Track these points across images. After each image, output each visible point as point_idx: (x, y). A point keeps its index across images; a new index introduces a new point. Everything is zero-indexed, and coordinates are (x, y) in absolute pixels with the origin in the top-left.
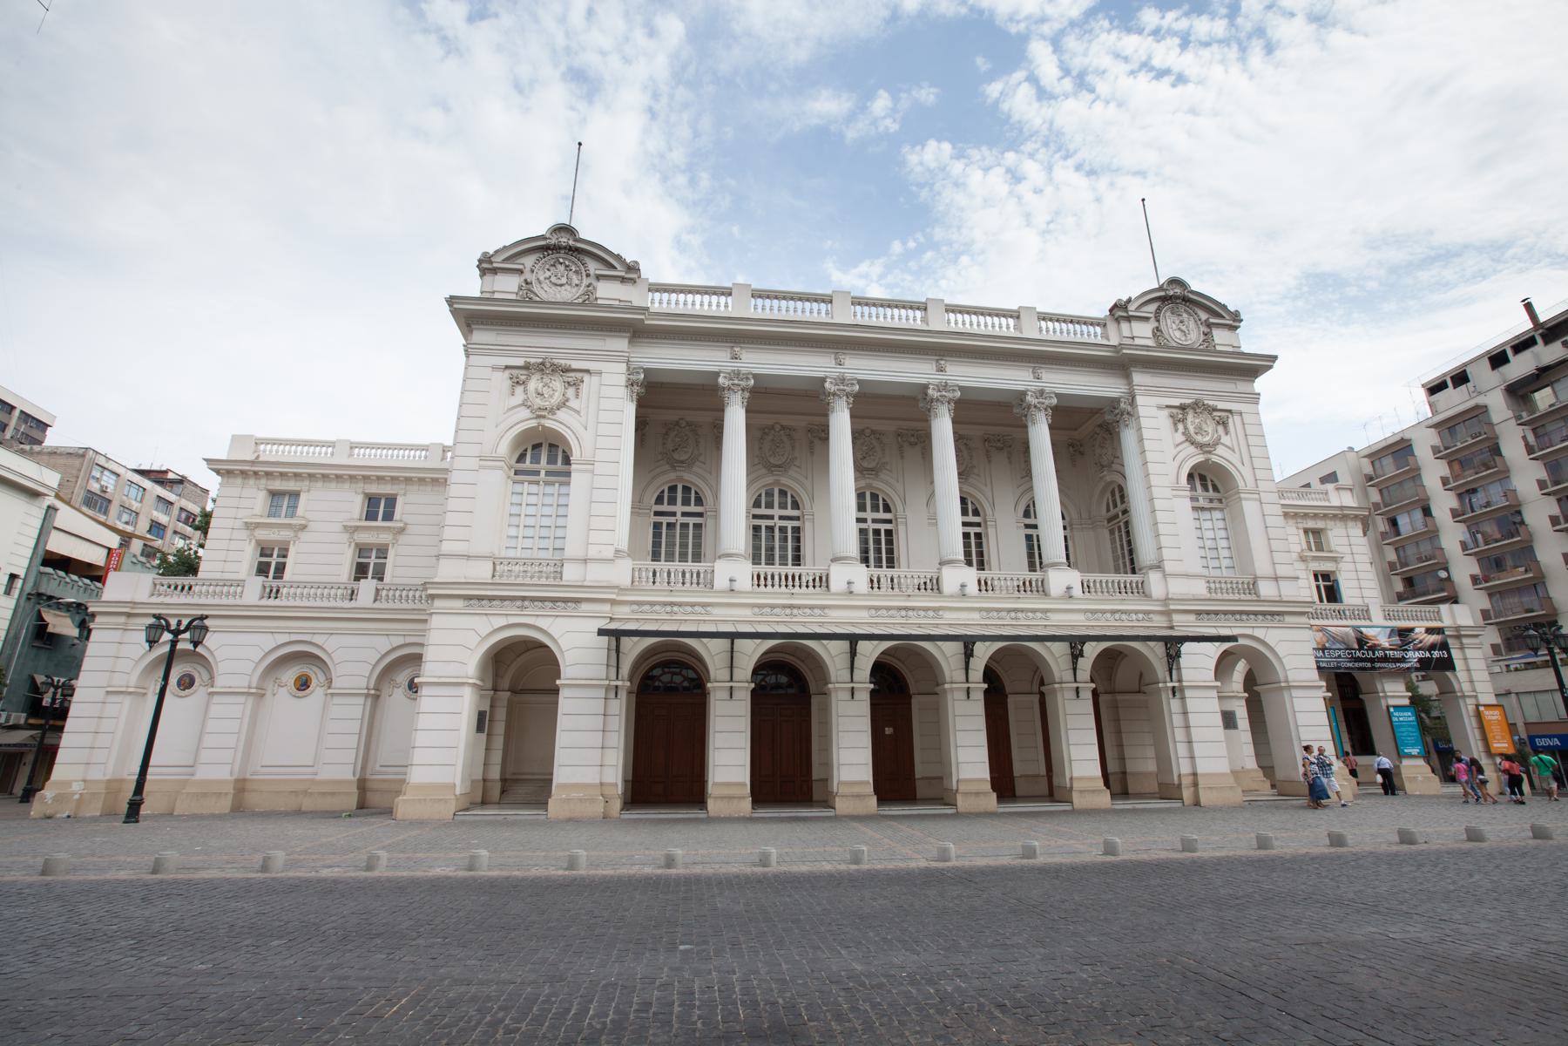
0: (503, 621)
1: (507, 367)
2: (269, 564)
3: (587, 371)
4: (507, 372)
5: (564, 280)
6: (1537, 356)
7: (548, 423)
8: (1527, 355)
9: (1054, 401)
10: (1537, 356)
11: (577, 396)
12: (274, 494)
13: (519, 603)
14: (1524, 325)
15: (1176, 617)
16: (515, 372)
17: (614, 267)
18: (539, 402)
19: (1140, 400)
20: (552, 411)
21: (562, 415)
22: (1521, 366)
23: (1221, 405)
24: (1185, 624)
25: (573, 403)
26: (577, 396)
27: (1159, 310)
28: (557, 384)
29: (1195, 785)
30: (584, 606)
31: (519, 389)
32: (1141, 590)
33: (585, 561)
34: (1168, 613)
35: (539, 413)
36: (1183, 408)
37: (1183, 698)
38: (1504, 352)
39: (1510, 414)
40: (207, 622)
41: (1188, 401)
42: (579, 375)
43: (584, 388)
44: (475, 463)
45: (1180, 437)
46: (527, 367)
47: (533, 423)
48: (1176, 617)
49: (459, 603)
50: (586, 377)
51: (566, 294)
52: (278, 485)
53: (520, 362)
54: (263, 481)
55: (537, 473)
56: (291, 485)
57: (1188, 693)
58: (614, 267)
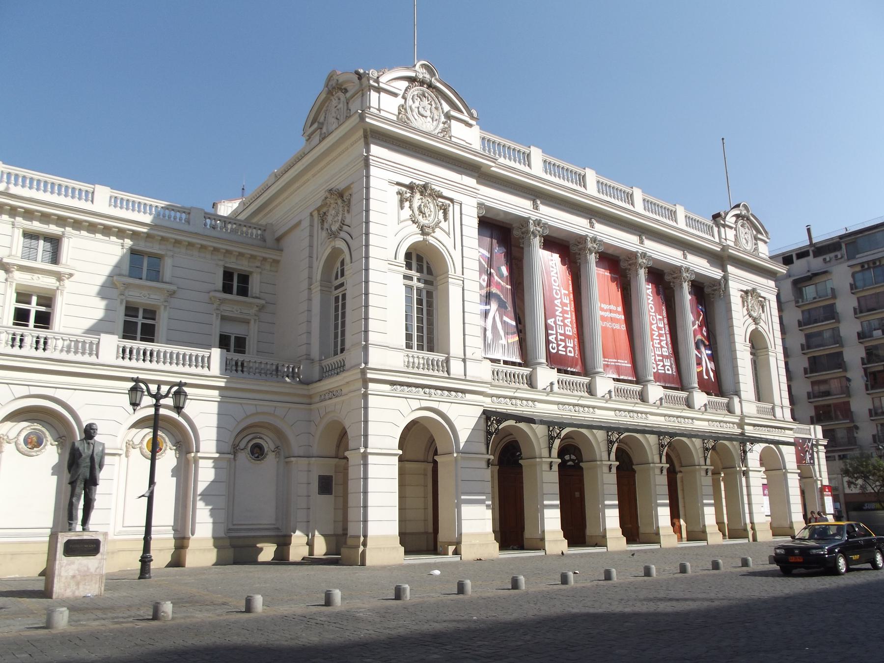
1: (398, 184)
2: (27, 312)
3: (452, 200)
5: (428, 113)
6: (808, 263)
7: (430, 239)
8: (803, 261)
9: (693, 277)
10: (808, 263)
11: (446, 219)
12: (30, 235)
14: (802, 241)
15: (746, 427)
16: (404, 189)
17: (461, 112)
19: (731, 284)
21: (438, 233)
22: (801, 267)
23: (763, 294)
24: (749, 431)
25: (444, 225)
26: (446, 219)
27: (736, 222)
28: (431, 207)
29: (753, 528)
32: (730, 410)
33: (464, 360)
34: (741, 425)
35: (423, 230)
36: (746, 292)
37: (747, 478)
38: (791, 256)
39: (793, 298)
40: (185, 389)
41: (750, 288)
42: (448, 202)
44: (385, 266)
45: (746, 312)
46: (411, 187)
47: (420, 238)
48: (746, 427)
49: (387, 387)
51: (427, 125)
52: (36, 226)
53: (407, 181)
54: (19, 219)
56: (53, 229)
57: (751, 473)
58: (461, 112)
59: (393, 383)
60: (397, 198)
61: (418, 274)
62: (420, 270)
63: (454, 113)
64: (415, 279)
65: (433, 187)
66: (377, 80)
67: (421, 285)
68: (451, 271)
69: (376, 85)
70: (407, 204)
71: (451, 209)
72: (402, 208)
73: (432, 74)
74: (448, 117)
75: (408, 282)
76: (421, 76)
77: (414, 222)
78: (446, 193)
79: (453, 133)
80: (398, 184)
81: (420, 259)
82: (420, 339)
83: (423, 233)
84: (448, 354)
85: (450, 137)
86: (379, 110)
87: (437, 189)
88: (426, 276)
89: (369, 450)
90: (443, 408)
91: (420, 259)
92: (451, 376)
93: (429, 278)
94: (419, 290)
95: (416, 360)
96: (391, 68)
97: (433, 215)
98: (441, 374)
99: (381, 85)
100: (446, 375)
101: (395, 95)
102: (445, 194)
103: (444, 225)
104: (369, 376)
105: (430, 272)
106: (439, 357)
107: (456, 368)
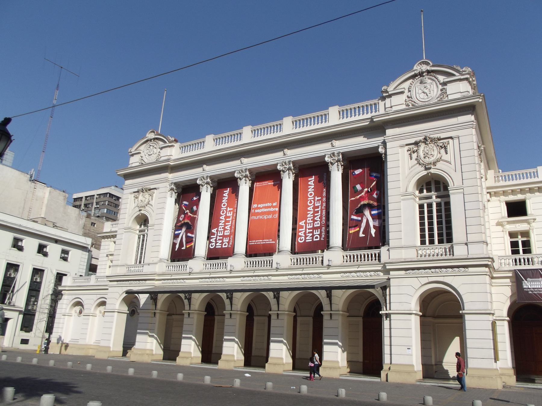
0: (425, 280)
1: (407, 145)
3: (451, 138)
4: (407, 148)
11: (446, 153)
13: (433, 270)
17: (454, 75)
18: (427, 160)
20: (434, 164)
21: (439, 165)
26: (446, 153)
30: (471, 269)
31: (414, 156)
43: (450, 148)
46: (416, 144)
47: (425, 173)
50: (450, 140)
53: (413, 141)
55: (430, 198)
58: (454, 75)
59: (406, 269)
61: (436, 193)
62: (437, 190)
64: (434, 197)
65: (431, 136)
66: (387, 92)
67: (439, 200)
69: (387, 94)
73: (427, 64)
77: (420, 164)
78: (443, 136)
80: (407, 145)
82: (440, 235)
83: (426, 169)
85: (447, 96)
87: (436, 136)
88: (442, 193)
94: (439, 205)
96: (394, 79)
97: (435, 153)
101: (402, 93)
102: (442, 137)
104: (387, 267)
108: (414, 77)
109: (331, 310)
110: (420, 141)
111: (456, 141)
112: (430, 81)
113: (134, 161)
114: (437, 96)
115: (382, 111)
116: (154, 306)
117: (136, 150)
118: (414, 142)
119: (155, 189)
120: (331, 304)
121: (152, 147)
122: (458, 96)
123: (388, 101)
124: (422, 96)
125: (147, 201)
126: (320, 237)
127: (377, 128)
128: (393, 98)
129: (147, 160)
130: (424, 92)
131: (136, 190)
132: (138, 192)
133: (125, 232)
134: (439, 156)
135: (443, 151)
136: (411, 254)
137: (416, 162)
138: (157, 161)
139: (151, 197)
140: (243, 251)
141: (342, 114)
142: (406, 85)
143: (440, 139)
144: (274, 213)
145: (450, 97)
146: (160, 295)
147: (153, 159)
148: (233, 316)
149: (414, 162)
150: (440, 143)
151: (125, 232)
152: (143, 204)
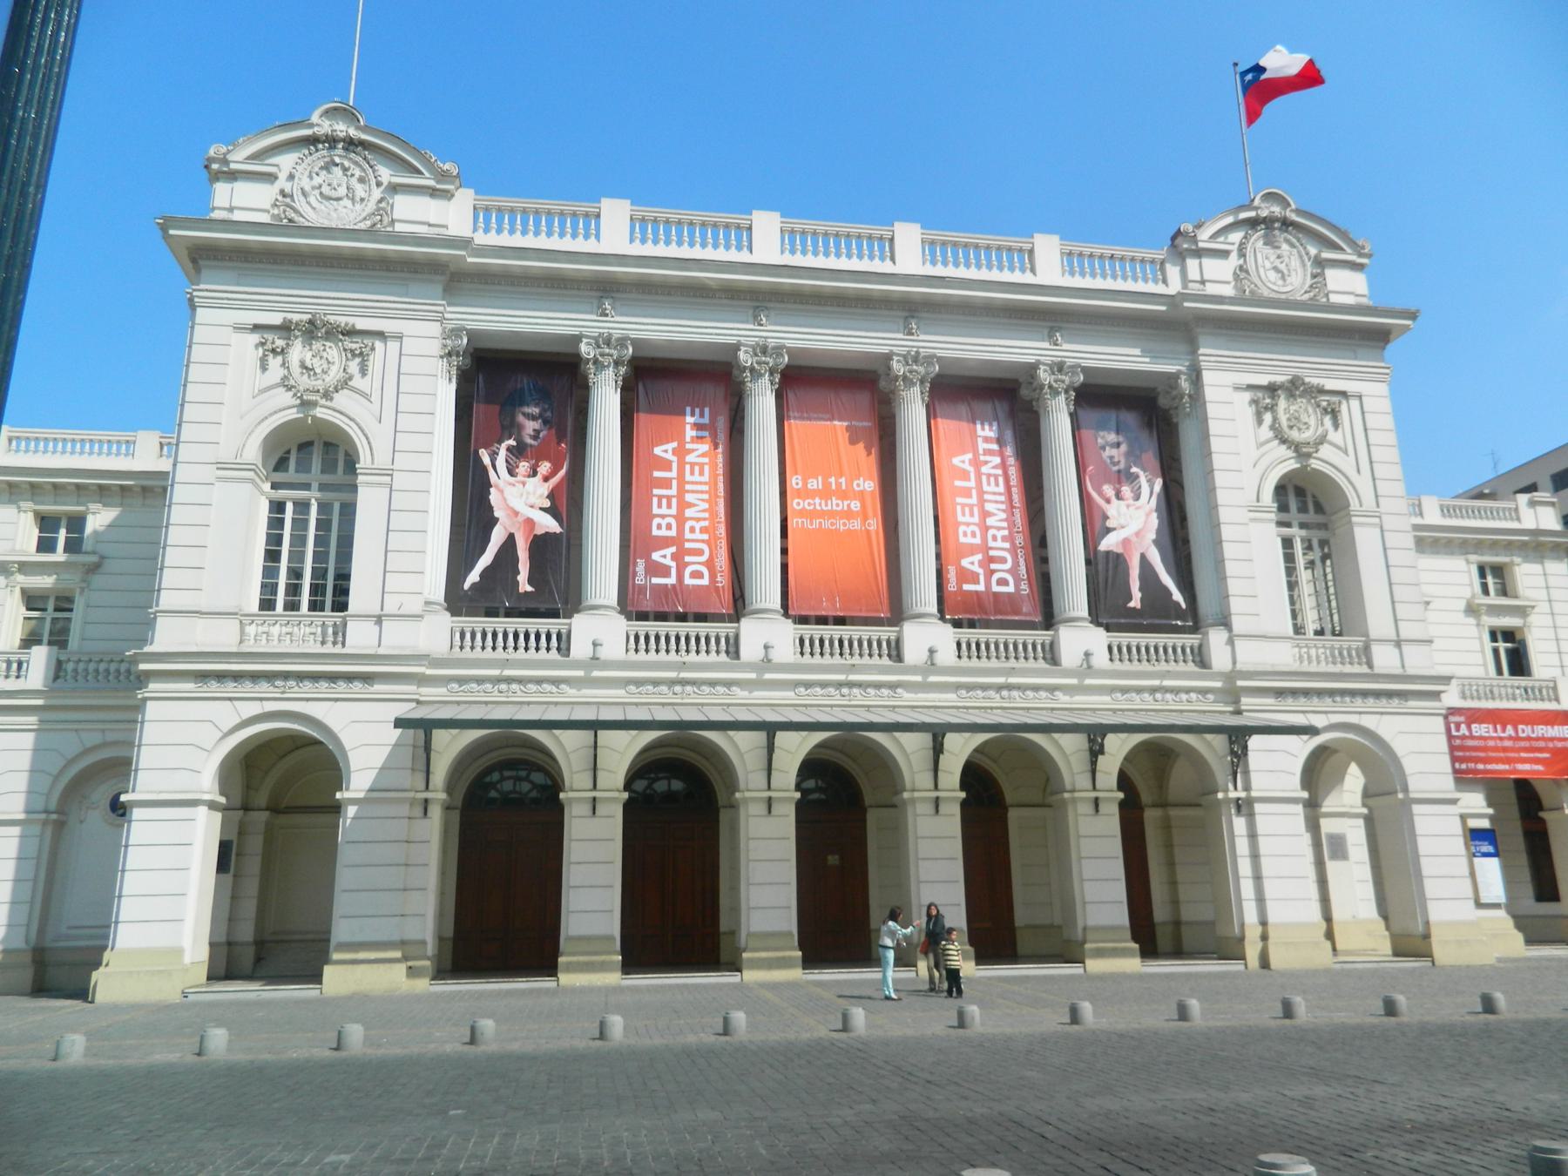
3: (1344, 394)
7: (1315, 464)
11: (1336, 425)
16: (1260, 395)
21: (1325, 451)
42: (1335, 399)
44: (1245, 515)
46: (1272, 389)
47: (1293, 465)
60: (1250, 412)
63: (1327, 255)
68: (1354, 504)
70: (1268, 417)
71: (1344, 407)
72: (1260, 422)
74: (1320, 263)
75: (1286, 531)
76: (1264, 213)
78: (1330, 385)
79: (1331, 286)
81: (1300, 492)
84: (1367, 635)
86: (1203, 282)
87: (1315, 381)
88: (1311, 517)
89: (1254, 794)
90: (1368, 722)
91: (1300, 492)
92: (1377, 670)
93: (1320, 519)
95: (1313, 652)
97: (1311, 424)
98: (1356, 669)
99: (1201, 245)
100: (1365, 669)
101: (1225, 254)
102: (1328, 387)
103: (1334, 436)
105: (1319, 509)
106: (1355, 642)
107: (1385, 658)
108: (1253, 223)
109: (1094, 788)
110: (1281, 387)
111: (1355, 403)
112: (1285, 246)
113: (244, 203)
114: (1306, 287)
115: (1174, 287)
116: (421, 777)
117: (256, 157)
118: (1265, 383)
119: (380, 335)
120: (1094, 772)
121: (337, 171)
122: (1349, 300)
123: (1192, 264)
124: (1272, 275)
125: (335, 374)
126: (713, 576)
127: (1180, 326)
128: (1206, 262)
129: (314, 213)
130: (1276, 269)
131: (276, 319)
132: (285, 329)
133: (219, 478)
134: (1320, 430)
135: (1328, 420)
136: (1283, 656)
137: (1271, 434)
138: (371, 234)
139: (354, 366)
140: (611, 596)
141: (640, 225)
142: (1236, 237)
143: (1322, 391)
144: (805, 493)
145: (1334, 298)
146: (440, 737)
147: (347, 215)
148: (600, 809)
149: (1265, 432)
150: (1324, 400)
151: (219, 478)
152: (319, 384)
